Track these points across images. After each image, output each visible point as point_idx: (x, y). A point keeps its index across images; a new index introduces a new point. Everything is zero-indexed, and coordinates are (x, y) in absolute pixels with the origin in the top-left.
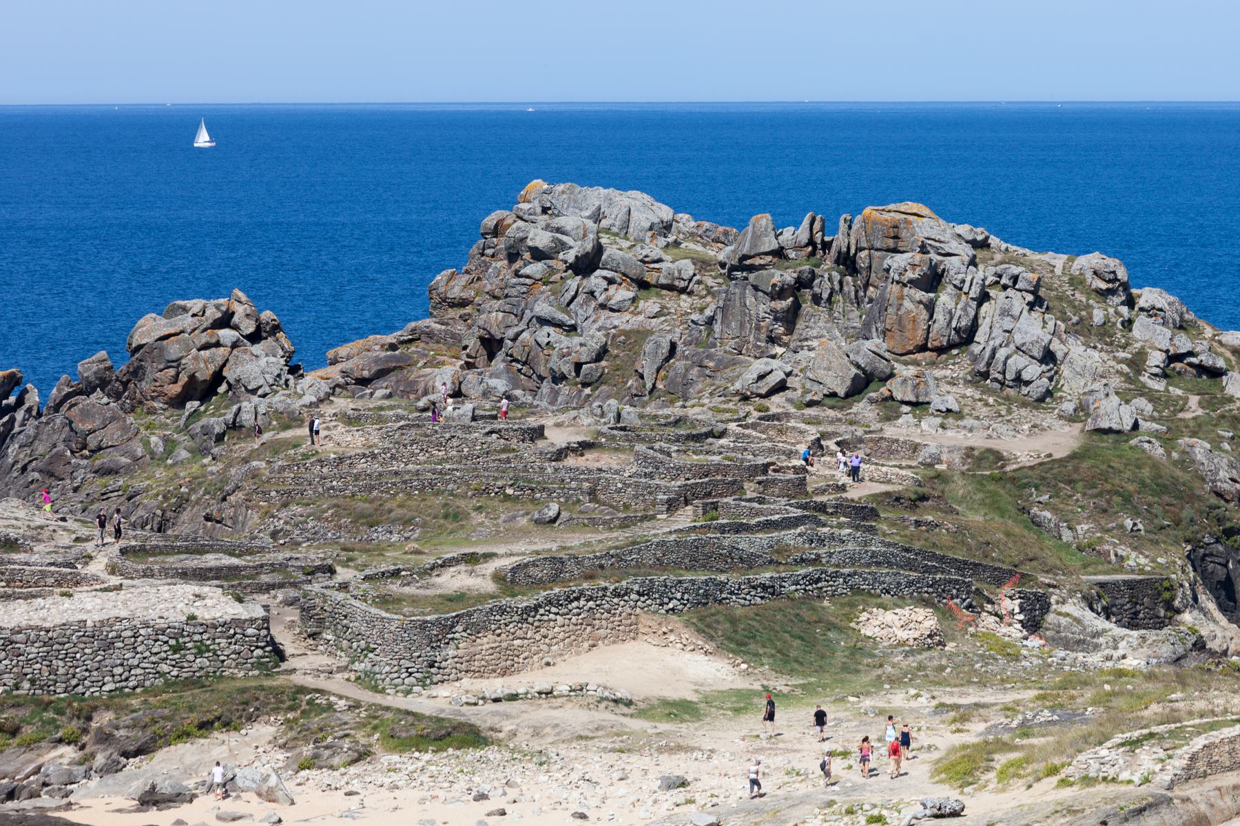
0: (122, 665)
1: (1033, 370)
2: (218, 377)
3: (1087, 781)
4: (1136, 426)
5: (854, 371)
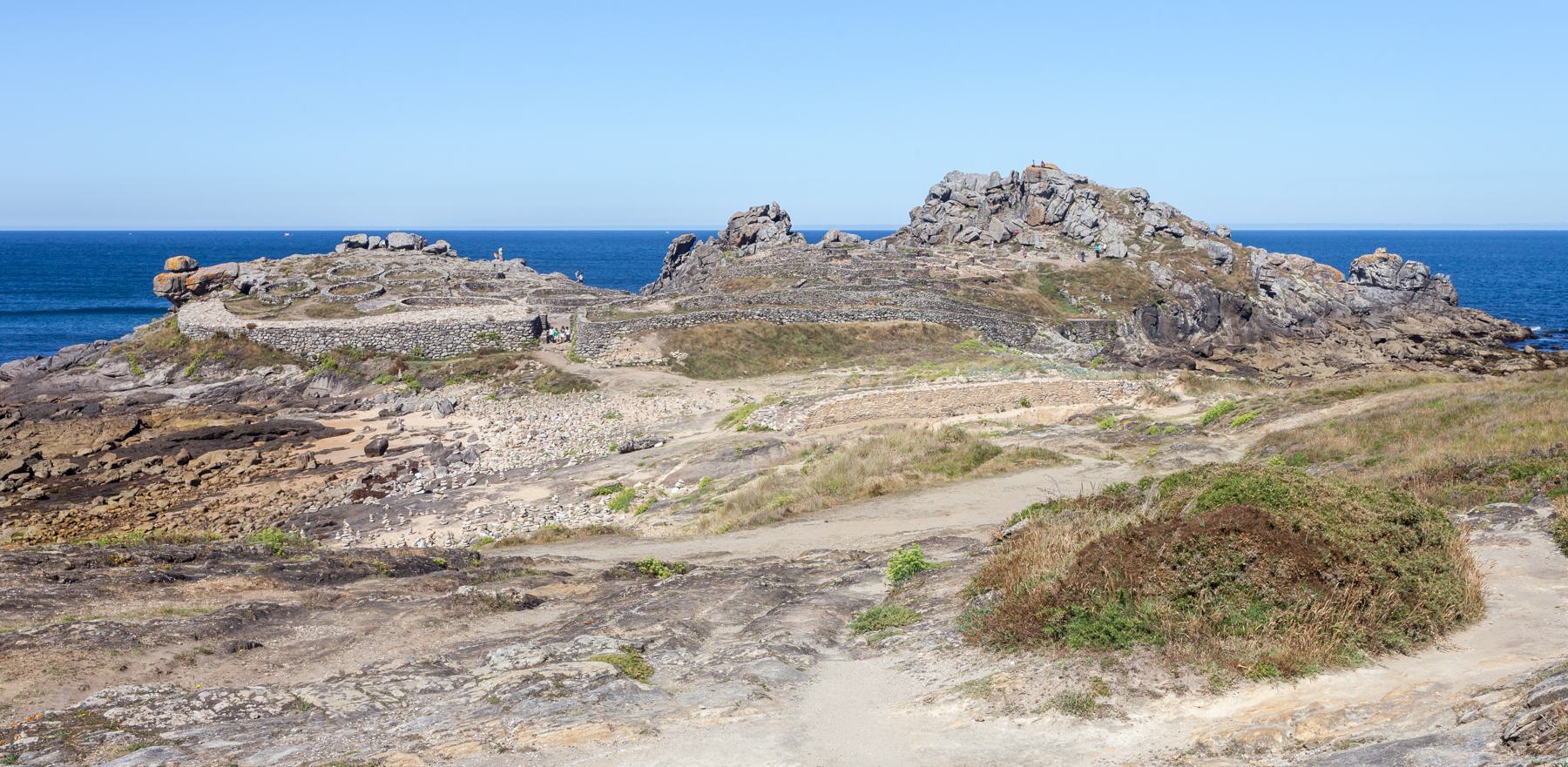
1: (1086, 231)
2: (755, 236)
3: (757, 429)
4: (1126, 255)
5: (1005, 231)
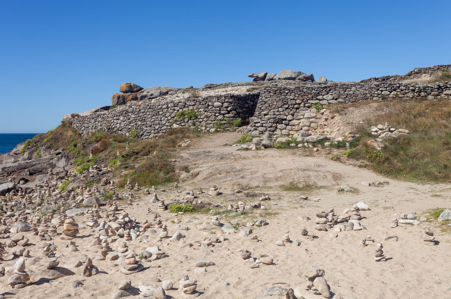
0: (159, 124)
